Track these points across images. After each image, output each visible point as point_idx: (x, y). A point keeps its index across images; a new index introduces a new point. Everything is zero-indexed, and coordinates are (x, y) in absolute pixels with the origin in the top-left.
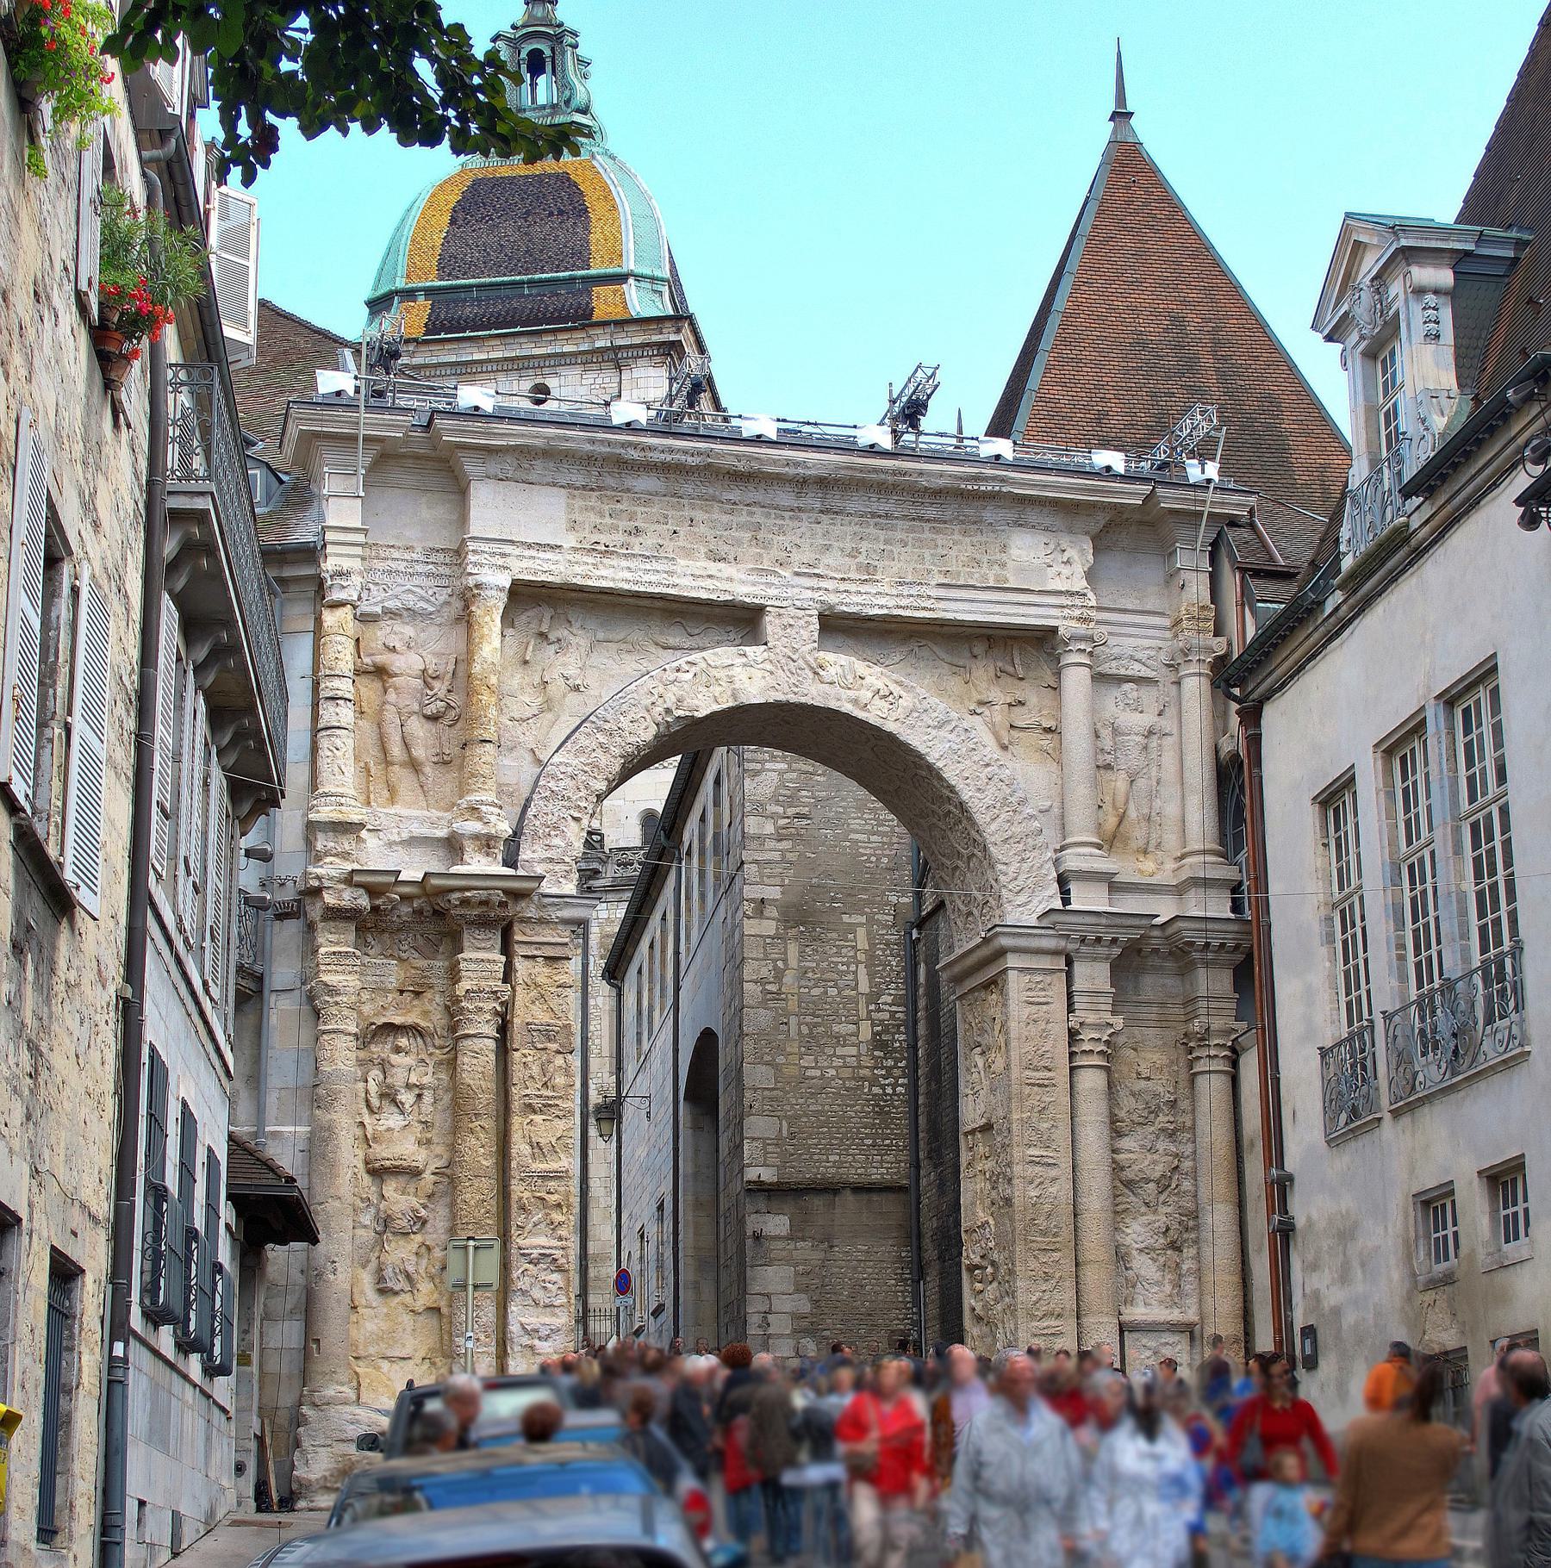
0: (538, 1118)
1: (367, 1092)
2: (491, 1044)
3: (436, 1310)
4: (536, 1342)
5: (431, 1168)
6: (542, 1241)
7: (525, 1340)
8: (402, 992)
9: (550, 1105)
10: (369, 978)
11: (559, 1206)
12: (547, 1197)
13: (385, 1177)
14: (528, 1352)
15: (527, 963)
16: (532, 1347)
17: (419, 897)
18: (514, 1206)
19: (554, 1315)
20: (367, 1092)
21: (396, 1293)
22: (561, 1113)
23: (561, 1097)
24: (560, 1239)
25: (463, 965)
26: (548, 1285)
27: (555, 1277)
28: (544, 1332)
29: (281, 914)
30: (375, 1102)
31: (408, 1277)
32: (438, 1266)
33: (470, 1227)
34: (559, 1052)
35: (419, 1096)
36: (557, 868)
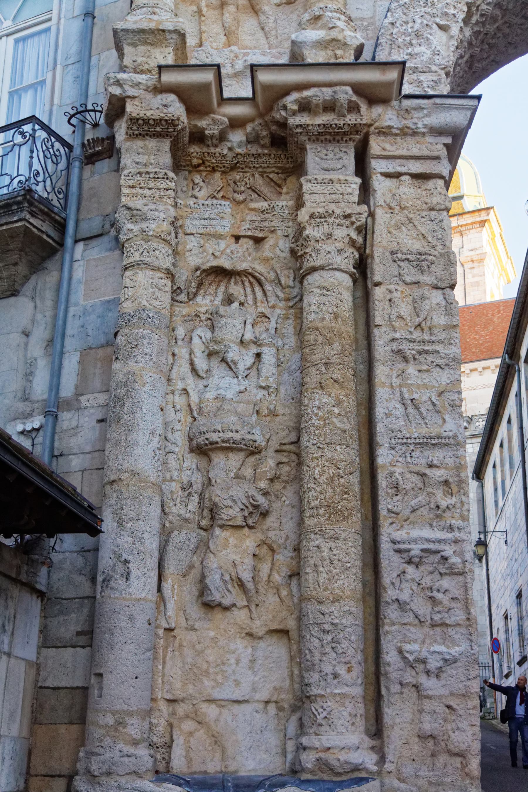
0: (411, 370)
1: (191, 352)
2: (347, 281)
3: (284, 632)
4: (423, 679)
5: (274, 444)
6: (427, 533)
7: (409, 677)
8: (237, 238)
9: (427, 352)
10: (195, 222)
11: (446, 483)
12: (428, 471)
13: (213, 455)
14: (410, 693)
15: (388, 183)
16: (416, 687)
17: (252, 120)
18: (383, 483)
19: (445, 640)
20: (191, 352)
21: (227, 609)
22: (442, 362)
23: (440, 342)
24: (451, 528)
25: (307, 187)
26: (439, 596)
27: (445, 583)
28: (434, 663)
29: (93, 155)
30: (201, 364)
31: (242, 585)
32: (285, 571)
33: (321, 512)
34: (436, 287)
35: (258, 356)
36: (422, 77)
